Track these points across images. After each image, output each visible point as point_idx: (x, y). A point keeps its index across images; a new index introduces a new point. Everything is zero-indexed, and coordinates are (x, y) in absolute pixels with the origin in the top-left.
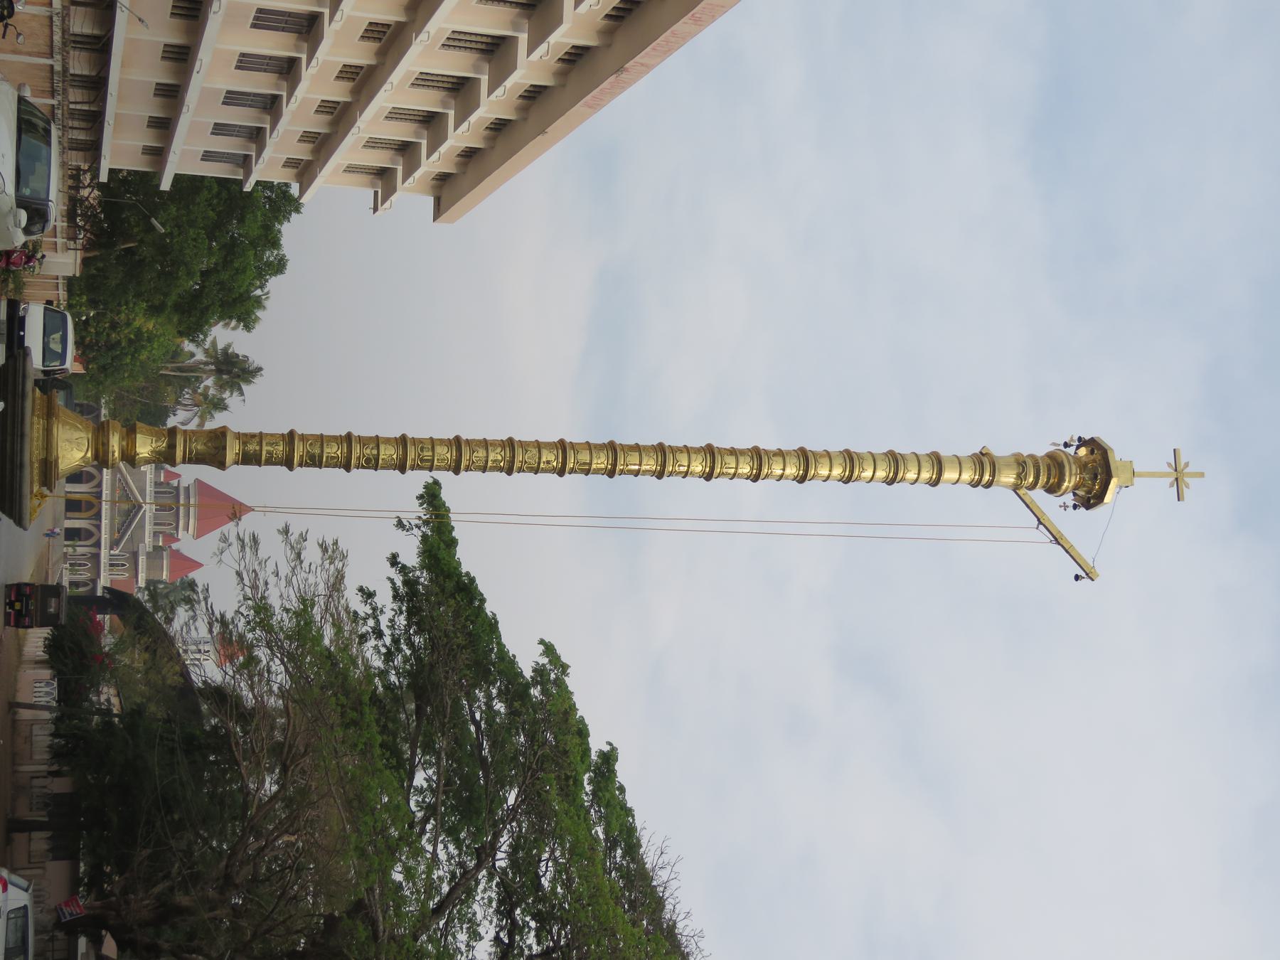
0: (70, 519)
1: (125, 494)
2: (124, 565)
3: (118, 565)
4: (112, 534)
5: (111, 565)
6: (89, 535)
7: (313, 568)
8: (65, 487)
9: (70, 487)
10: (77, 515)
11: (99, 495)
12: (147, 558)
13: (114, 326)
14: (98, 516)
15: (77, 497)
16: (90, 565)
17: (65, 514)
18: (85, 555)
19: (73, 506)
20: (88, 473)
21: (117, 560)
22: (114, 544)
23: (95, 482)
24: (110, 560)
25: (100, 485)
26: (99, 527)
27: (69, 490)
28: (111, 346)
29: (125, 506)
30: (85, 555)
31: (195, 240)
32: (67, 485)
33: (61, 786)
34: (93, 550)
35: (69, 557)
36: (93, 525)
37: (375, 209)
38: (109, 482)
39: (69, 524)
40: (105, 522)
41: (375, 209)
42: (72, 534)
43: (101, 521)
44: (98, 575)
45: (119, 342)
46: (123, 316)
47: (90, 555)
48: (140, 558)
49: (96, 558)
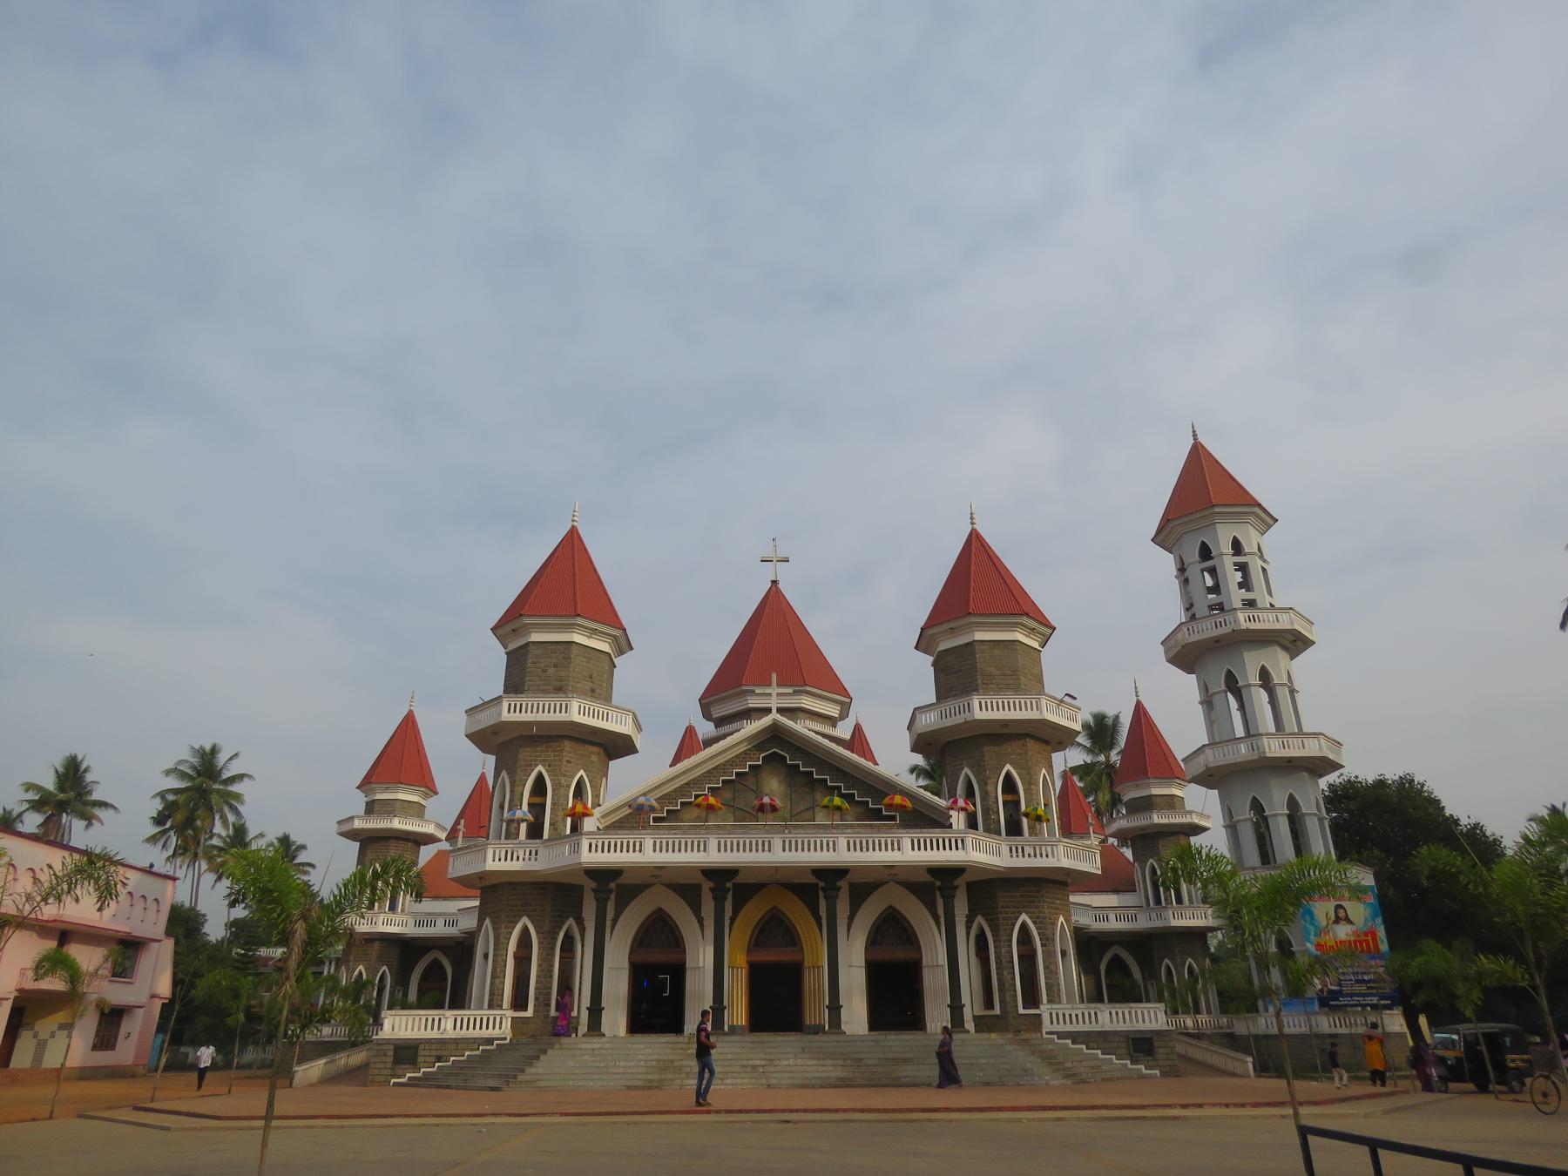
0: (835, 1008)
1: (727, 795)
3: (1012, 805)
5: (1014, 829)
10: (815, 982)
12: (976, 690)
16: (1024, 917)
17: (817, 1030)
24: (992, 829)
29: (774, 788)
35: (997, 1011)
36: (851, 919)
39: (856, 1013)
47: (980, 919)
48: (979, 715)
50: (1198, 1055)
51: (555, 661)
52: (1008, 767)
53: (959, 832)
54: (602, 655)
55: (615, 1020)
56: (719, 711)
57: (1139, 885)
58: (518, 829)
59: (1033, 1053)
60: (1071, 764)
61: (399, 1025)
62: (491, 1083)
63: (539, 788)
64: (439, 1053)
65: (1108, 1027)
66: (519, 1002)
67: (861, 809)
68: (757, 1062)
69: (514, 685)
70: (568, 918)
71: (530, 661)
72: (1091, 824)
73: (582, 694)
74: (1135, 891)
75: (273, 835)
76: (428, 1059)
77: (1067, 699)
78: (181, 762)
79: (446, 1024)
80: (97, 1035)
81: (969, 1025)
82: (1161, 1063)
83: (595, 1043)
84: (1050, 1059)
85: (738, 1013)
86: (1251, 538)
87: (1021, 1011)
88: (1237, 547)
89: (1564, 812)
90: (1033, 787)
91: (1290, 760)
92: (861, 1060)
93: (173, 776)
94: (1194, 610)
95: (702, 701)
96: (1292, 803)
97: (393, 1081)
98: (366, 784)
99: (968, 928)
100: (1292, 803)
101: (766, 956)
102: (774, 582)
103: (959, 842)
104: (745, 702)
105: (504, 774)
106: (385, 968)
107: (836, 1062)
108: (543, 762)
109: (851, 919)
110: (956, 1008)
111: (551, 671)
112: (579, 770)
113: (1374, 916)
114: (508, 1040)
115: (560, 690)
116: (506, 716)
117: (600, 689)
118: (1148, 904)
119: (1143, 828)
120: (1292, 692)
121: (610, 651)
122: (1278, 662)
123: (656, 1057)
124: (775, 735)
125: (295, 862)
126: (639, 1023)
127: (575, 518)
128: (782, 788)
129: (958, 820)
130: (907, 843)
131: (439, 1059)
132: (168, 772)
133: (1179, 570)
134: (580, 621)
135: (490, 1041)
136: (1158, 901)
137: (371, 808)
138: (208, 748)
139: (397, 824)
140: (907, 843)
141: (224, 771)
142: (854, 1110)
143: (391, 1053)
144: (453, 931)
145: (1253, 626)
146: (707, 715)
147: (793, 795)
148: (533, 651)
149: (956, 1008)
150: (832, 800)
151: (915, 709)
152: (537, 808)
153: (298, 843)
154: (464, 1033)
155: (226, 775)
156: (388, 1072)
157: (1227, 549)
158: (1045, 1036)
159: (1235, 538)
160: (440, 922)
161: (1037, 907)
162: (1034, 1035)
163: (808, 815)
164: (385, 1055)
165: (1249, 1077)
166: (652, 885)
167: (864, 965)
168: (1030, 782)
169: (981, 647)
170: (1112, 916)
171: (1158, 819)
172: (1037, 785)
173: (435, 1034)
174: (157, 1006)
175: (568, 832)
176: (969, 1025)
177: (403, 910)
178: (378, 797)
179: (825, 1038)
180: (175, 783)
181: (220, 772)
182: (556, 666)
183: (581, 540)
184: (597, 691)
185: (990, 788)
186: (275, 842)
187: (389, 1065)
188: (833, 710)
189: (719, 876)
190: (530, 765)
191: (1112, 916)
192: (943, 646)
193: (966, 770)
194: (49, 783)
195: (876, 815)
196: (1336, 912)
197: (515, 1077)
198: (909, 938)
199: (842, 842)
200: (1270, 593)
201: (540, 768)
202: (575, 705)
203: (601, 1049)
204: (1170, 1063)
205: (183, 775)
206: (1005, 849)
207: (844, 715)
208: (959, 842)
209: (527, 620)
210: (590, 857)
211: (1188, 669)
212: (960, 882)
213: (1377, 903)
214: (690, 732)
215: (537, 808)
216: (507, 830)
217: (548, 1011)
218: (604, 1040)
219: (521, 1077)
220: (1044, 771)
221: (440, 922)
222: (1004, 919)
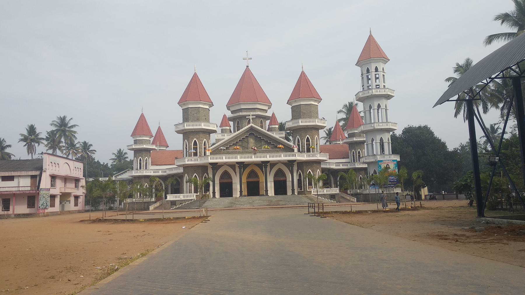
0: (267, 191)
1: (240, 143)
2: (308, 140)
3: (308, 145)
5: (308, 151)
6: (280, 173)
8: (236, 198)
9: (237, 193)
10: (262, 185)
11: (243, 165)
12: (301, 118)
14: (263, 165)
15: (244, 187)
17: (263, 195)
18: (300, 175)
20: (221, 178)
24: (303, 151)
25: (232, 166)
26: (273, 164)
27: (239, 193)
29: (251, 141)
30: (300, 175)
32: (234, 196)
34: (295, 168)
36: (270, 171)
38: (228, 156)
39: (271, 192)
40: (268, 158)
43: (268, 162)
44: (319, 162)
47: (300, 171)
48: (301, 124)
49: (302, 165)
50: (348, 198)
51: (196, 112)
52: (308, 136)
53: (296, 153)
54: (207, 109)
55: (217, 195)
56: (233, 109)
57: (350, 157)
58: (191, 154)
59: (308, 199)
60: (339, 118)
61: (171, 197)
62: (197, 208)
63: (195, 143)
64: (181, 203)
65: (326, 193)
66: (196, 192)
67: (273, 146)
68: (251, 202)
69: (186, 119)
70: (205, 173)
71: (189, 112)
72: (341, 138)
73: (204, 121)
74: (349, 158)
75: (82, 141)
76: (178, 204)
77: (323, 119)
78: (53, 121)
79: (181, 197)
80: (75, 203)
81: (296, 193)
82: (337, 200)
83: (214, 199)
85: (245, 192)
86: (380, 66)
87: (308, 190)
88: (376, 70)
89: (494, 127)
90: (313, 140)
91: (382, 129)
92: (272, 201)
93: (53, 126)
94: (364, 87)
95: (227, 106)
96: (381, 140)
97: (171, 208)
98: (133, 135)
99: (297, 173)
100: (381, 140)
101: (251, 180)
102: (247, 66)
103: (294, 155)
104: (240, 107)
105: (186, 140)
106: (146, 184)
107: (267, 201)
108: (196, 138)
109: (270, 171)
110: (293, 190)
111: (195, 115)
112: (204, 139)
113: (395, 167)
114: (196, 200)
115: (198, 120)
116: (186, 127)
117: (207, 120)
118: (351, 162)
119: (352, 142)
120: (386, 110)
121: (209, 108)
122: (383, 103)
123: (229, 202)
124: (251, 126)
125: (89, 150)
126: (221, 196)
127: (195, 70)
128: (254, 141)
129: (296, 150)
130: (282, 155)
131: (181, 204)
132: (51, 125)
133: (361, 75)
134: (201, 102)
135: (192, 200)
136: (354, 161)
137: (136, 142)
138: (62, 116)
139: (145, 146)
140: (282, 155)
141: (68, 124)
142: (269, 208)
143: (170, 203)
144: (165, 174)
145: (376, 93)
146: (228, 108)
147: (256, 143)
148: (190, 110)
149: (293, 190)
150: (265, 146)
151: (286, 122)
152: (195, 149)
153: (89, 143)
154: (185, 198)
155: (69, 125)
156: (170, 207)
157: (373, 70)
158: (312, 195)
159: (376, 66)
160: (160, 171)
161: (313, 168)
162: (309, 195)
163: (260, 147)
164: (169, 203)
165: (355, 202)
166: (223, 165)
167: (273, 181)
168: (313, 139)
169: (303, 106)
170: (341, 165)
171: (355, 139)
172: (314, 140)
173: (179, 199)
174: (84, 195)
175: (203, 155)
176: (296, 193)
177: (149, 169)
178: (138, 139)
179: (264, 197)
180: (54, 128)
181: (67, 124)
182: (196, 113)
183: (198, 77)
184: (207, 119)
185: (303, 141)
186: (82, 144)
187: (170, 205)
188: (265, 108)
189: (240, 164)
190: (193, 139)
191: (341, 165)
192: (294, 105)
193: (298, 136)
194: (26, 133)
195: (276, 147)
196: (387, 165)
197: (201, 206)
198: (284, 175)
199: (268, 156)
200: (384, 82)
201: (195, 139)
202: (203, 124)
203: (217, 200)
204: (338, 200)
205: (56, 125)
206: (305, 156)
207: (270, 107)
208: (294, 155)
209: (188, 102)
210: (211, 160)
211: (362, 102)
212: (295, 164)
213: (397, 164)
214: (225, 116)
215: (195, 149)
216: (188, 154)
217: (202, 193)
218: (216, 199)
219: (202, 206)
220: (317, 136)
221: (160, 171)
222: (305, 171)
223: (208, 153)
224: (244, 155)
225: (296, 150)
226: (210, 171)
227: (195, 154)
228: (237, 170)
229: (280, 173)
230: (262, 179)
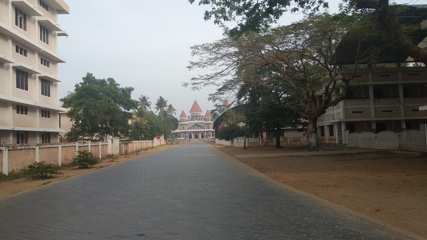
0: (199, 137)
3: (208, 127)
4: (202, 129)
5: (209, 128)
6: (202, 133)
7: (201, 58)
9: (193, 138)
10: (198, 136)
13: (147, 129)
14: (198, 132)
15: (194, 136)
19: (196, 137)
20: (189, 134)
21: (207, 127)
22: (204, 128)
23: (191, 133)
28: (152, 129)
29: (196, 126)
31: (100, 104)
33: (265, 134)
34: (206, 132)
37: (65, 35)
39: (200, 137)
40: (199, 130)
41: (65, 35)
42: (202, 137)
44: (211, 131)
45: (151, 128)
46: (144, 127)
61: (179, 139)
66: (184, 137)
79: (181, 138)
81: (206, 138)
84: (208, 139)
85: (194, 138)
152: (183, 128)
223: (186, 129)
224: (194, 130)
225: (206, 128)
226: (187, 133)
227: (184, 129)
228: (193, 133)
229: (202, 133)
230: (198, 135)
